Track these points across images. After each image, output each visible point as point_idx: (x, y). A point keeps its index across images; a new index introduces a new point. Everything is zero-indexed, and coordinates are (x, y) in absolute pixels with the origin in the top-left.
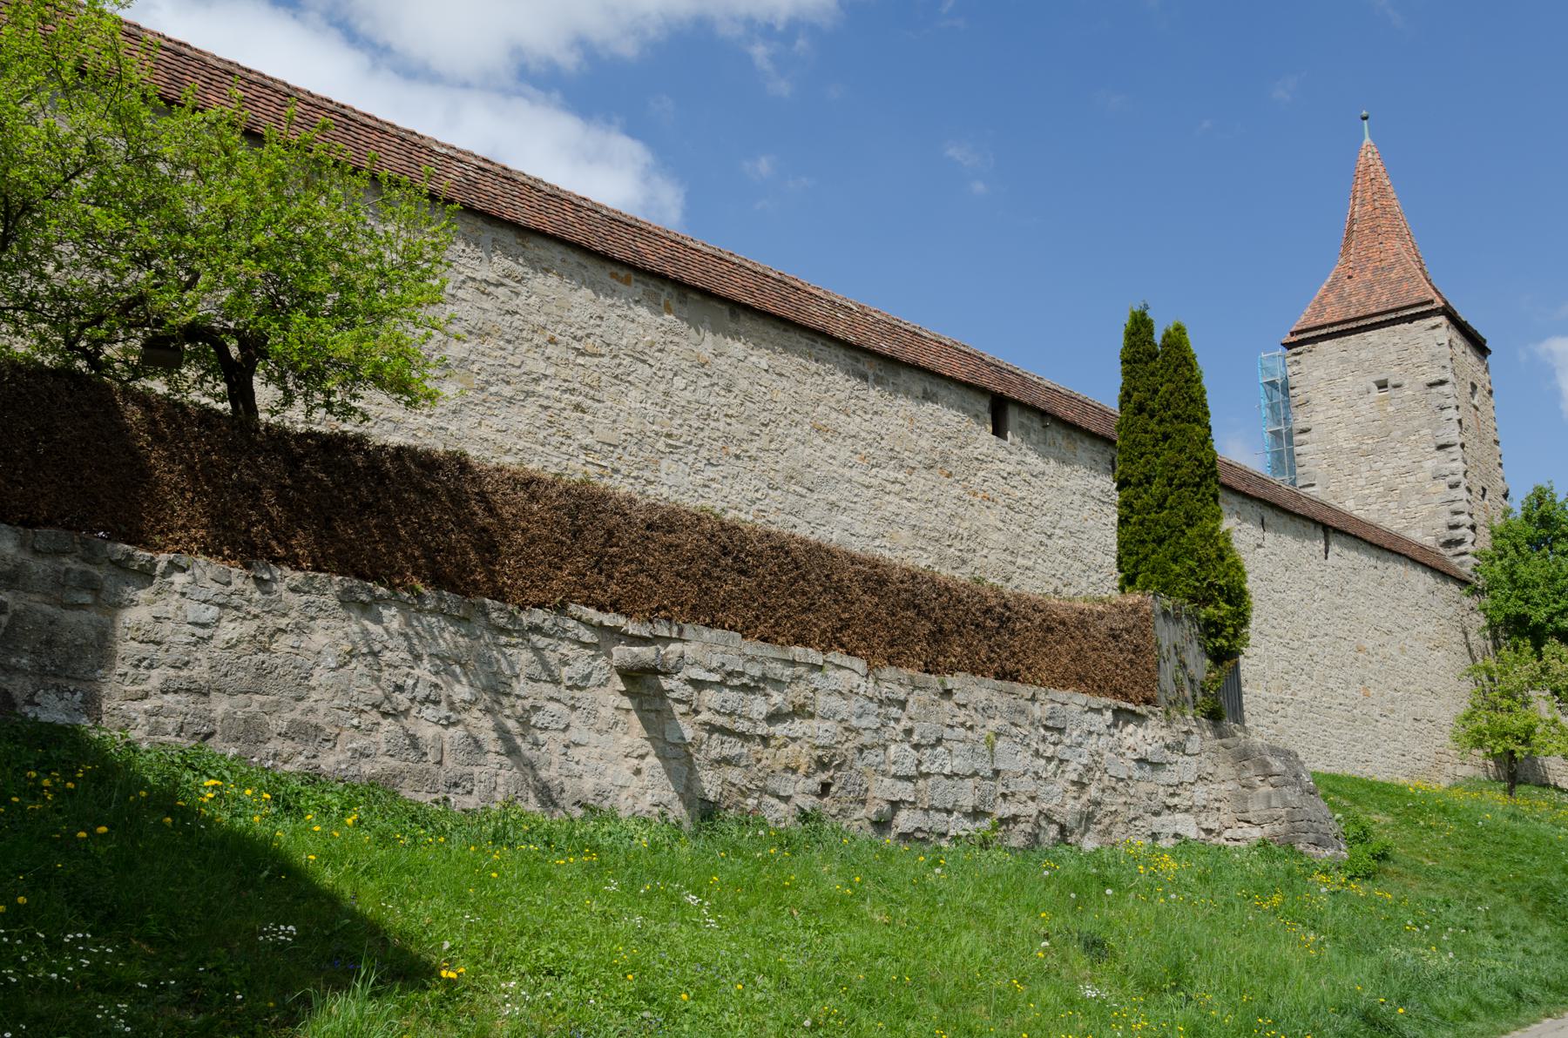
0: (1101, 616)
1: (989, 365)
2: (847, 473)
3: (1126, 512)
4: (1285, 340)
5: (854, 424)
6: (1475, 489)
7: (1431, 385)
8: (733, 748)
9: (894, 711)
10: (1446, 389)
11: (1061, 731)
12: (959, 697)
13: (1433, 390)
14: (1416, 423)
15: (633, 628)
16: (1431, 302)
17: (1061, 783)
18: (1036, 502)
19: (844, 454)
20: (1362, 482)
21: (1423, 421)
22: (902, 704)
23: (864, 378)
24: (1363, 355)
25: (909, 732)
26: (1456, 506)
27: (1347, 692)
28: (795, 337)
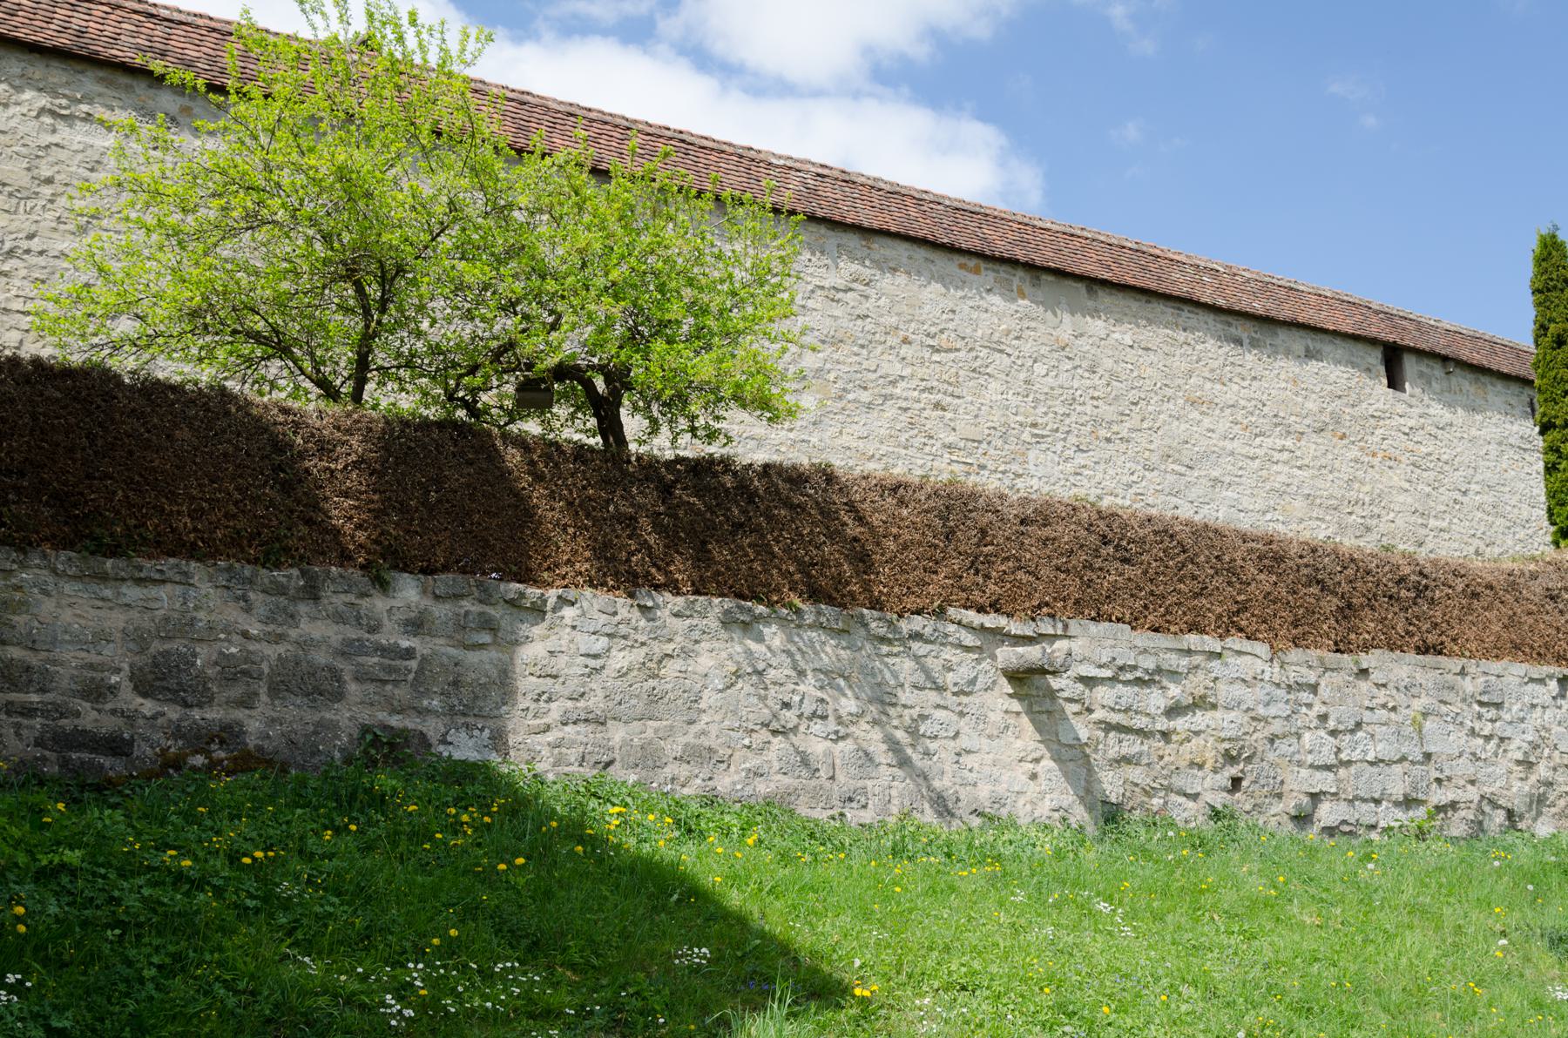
0: (1534, 576)
1: (1377, 312)
2: (1229, 445)
3: (1553, 457)
5: (1231, 393)
8: (1132, 746)
9: (1305, 696)
11: (1498, 706)
12: (1376, 676)
15: (1015, 627)
17: (1504, 765)
18: (1445, 457)
19: (1223, 426)
22: (1314, 688)
23: (1238, 342)
25: (1323, 718)
28: (1159, 307)
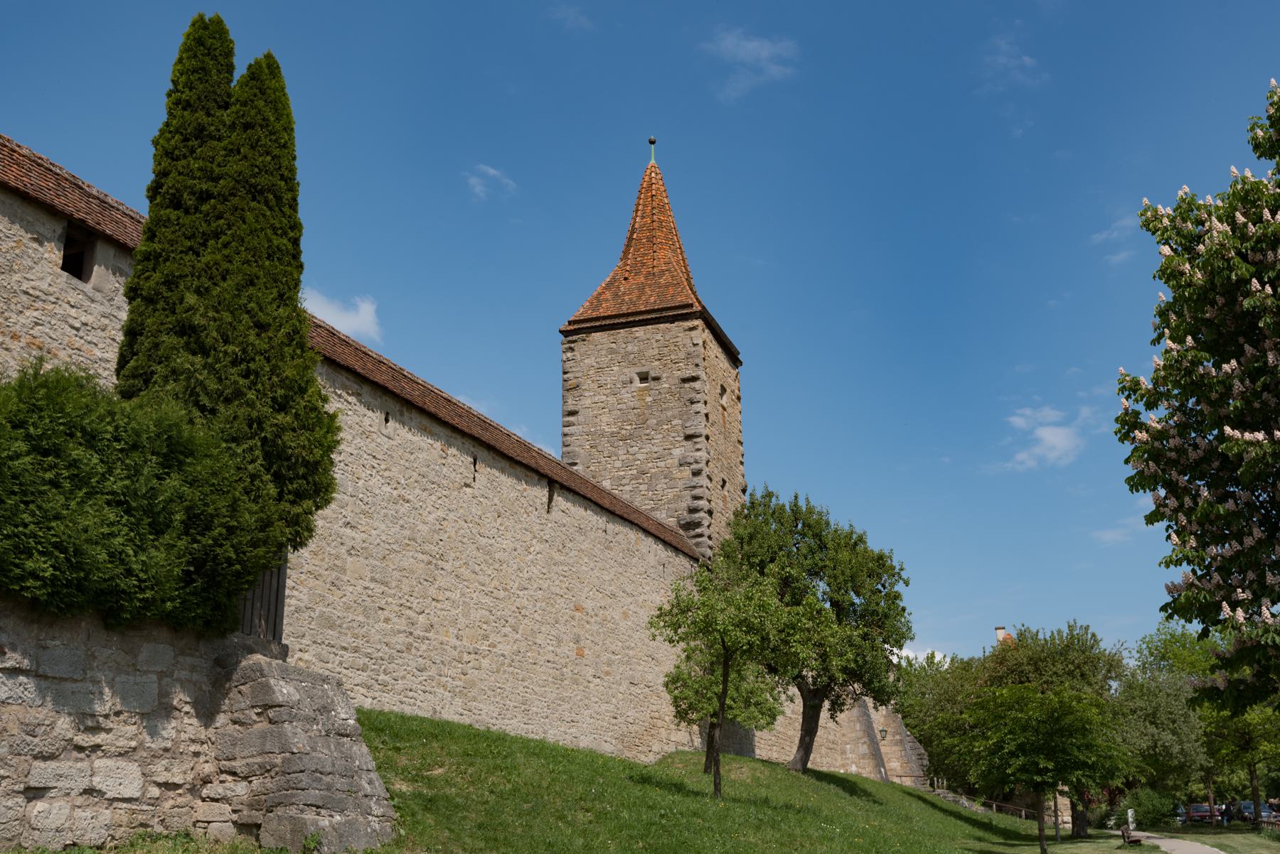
4: (563, 328)
6: (715, 479)
7: (685, 380)
10: (697, 385)
13: (687, 385)
14: (669, 413)
16: (691, 306)
20: (618, 464)
21: (676, 412)
24: (630, 348)
26: (697, 492)
27: (559, 651)
